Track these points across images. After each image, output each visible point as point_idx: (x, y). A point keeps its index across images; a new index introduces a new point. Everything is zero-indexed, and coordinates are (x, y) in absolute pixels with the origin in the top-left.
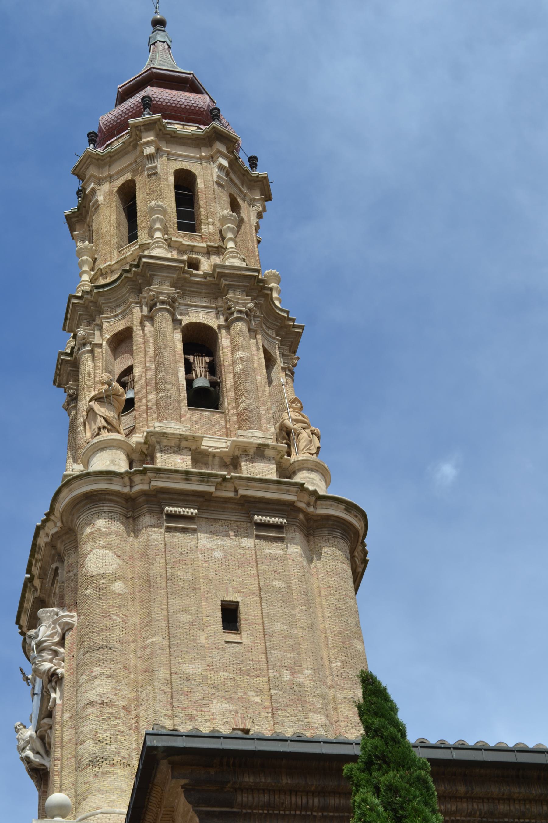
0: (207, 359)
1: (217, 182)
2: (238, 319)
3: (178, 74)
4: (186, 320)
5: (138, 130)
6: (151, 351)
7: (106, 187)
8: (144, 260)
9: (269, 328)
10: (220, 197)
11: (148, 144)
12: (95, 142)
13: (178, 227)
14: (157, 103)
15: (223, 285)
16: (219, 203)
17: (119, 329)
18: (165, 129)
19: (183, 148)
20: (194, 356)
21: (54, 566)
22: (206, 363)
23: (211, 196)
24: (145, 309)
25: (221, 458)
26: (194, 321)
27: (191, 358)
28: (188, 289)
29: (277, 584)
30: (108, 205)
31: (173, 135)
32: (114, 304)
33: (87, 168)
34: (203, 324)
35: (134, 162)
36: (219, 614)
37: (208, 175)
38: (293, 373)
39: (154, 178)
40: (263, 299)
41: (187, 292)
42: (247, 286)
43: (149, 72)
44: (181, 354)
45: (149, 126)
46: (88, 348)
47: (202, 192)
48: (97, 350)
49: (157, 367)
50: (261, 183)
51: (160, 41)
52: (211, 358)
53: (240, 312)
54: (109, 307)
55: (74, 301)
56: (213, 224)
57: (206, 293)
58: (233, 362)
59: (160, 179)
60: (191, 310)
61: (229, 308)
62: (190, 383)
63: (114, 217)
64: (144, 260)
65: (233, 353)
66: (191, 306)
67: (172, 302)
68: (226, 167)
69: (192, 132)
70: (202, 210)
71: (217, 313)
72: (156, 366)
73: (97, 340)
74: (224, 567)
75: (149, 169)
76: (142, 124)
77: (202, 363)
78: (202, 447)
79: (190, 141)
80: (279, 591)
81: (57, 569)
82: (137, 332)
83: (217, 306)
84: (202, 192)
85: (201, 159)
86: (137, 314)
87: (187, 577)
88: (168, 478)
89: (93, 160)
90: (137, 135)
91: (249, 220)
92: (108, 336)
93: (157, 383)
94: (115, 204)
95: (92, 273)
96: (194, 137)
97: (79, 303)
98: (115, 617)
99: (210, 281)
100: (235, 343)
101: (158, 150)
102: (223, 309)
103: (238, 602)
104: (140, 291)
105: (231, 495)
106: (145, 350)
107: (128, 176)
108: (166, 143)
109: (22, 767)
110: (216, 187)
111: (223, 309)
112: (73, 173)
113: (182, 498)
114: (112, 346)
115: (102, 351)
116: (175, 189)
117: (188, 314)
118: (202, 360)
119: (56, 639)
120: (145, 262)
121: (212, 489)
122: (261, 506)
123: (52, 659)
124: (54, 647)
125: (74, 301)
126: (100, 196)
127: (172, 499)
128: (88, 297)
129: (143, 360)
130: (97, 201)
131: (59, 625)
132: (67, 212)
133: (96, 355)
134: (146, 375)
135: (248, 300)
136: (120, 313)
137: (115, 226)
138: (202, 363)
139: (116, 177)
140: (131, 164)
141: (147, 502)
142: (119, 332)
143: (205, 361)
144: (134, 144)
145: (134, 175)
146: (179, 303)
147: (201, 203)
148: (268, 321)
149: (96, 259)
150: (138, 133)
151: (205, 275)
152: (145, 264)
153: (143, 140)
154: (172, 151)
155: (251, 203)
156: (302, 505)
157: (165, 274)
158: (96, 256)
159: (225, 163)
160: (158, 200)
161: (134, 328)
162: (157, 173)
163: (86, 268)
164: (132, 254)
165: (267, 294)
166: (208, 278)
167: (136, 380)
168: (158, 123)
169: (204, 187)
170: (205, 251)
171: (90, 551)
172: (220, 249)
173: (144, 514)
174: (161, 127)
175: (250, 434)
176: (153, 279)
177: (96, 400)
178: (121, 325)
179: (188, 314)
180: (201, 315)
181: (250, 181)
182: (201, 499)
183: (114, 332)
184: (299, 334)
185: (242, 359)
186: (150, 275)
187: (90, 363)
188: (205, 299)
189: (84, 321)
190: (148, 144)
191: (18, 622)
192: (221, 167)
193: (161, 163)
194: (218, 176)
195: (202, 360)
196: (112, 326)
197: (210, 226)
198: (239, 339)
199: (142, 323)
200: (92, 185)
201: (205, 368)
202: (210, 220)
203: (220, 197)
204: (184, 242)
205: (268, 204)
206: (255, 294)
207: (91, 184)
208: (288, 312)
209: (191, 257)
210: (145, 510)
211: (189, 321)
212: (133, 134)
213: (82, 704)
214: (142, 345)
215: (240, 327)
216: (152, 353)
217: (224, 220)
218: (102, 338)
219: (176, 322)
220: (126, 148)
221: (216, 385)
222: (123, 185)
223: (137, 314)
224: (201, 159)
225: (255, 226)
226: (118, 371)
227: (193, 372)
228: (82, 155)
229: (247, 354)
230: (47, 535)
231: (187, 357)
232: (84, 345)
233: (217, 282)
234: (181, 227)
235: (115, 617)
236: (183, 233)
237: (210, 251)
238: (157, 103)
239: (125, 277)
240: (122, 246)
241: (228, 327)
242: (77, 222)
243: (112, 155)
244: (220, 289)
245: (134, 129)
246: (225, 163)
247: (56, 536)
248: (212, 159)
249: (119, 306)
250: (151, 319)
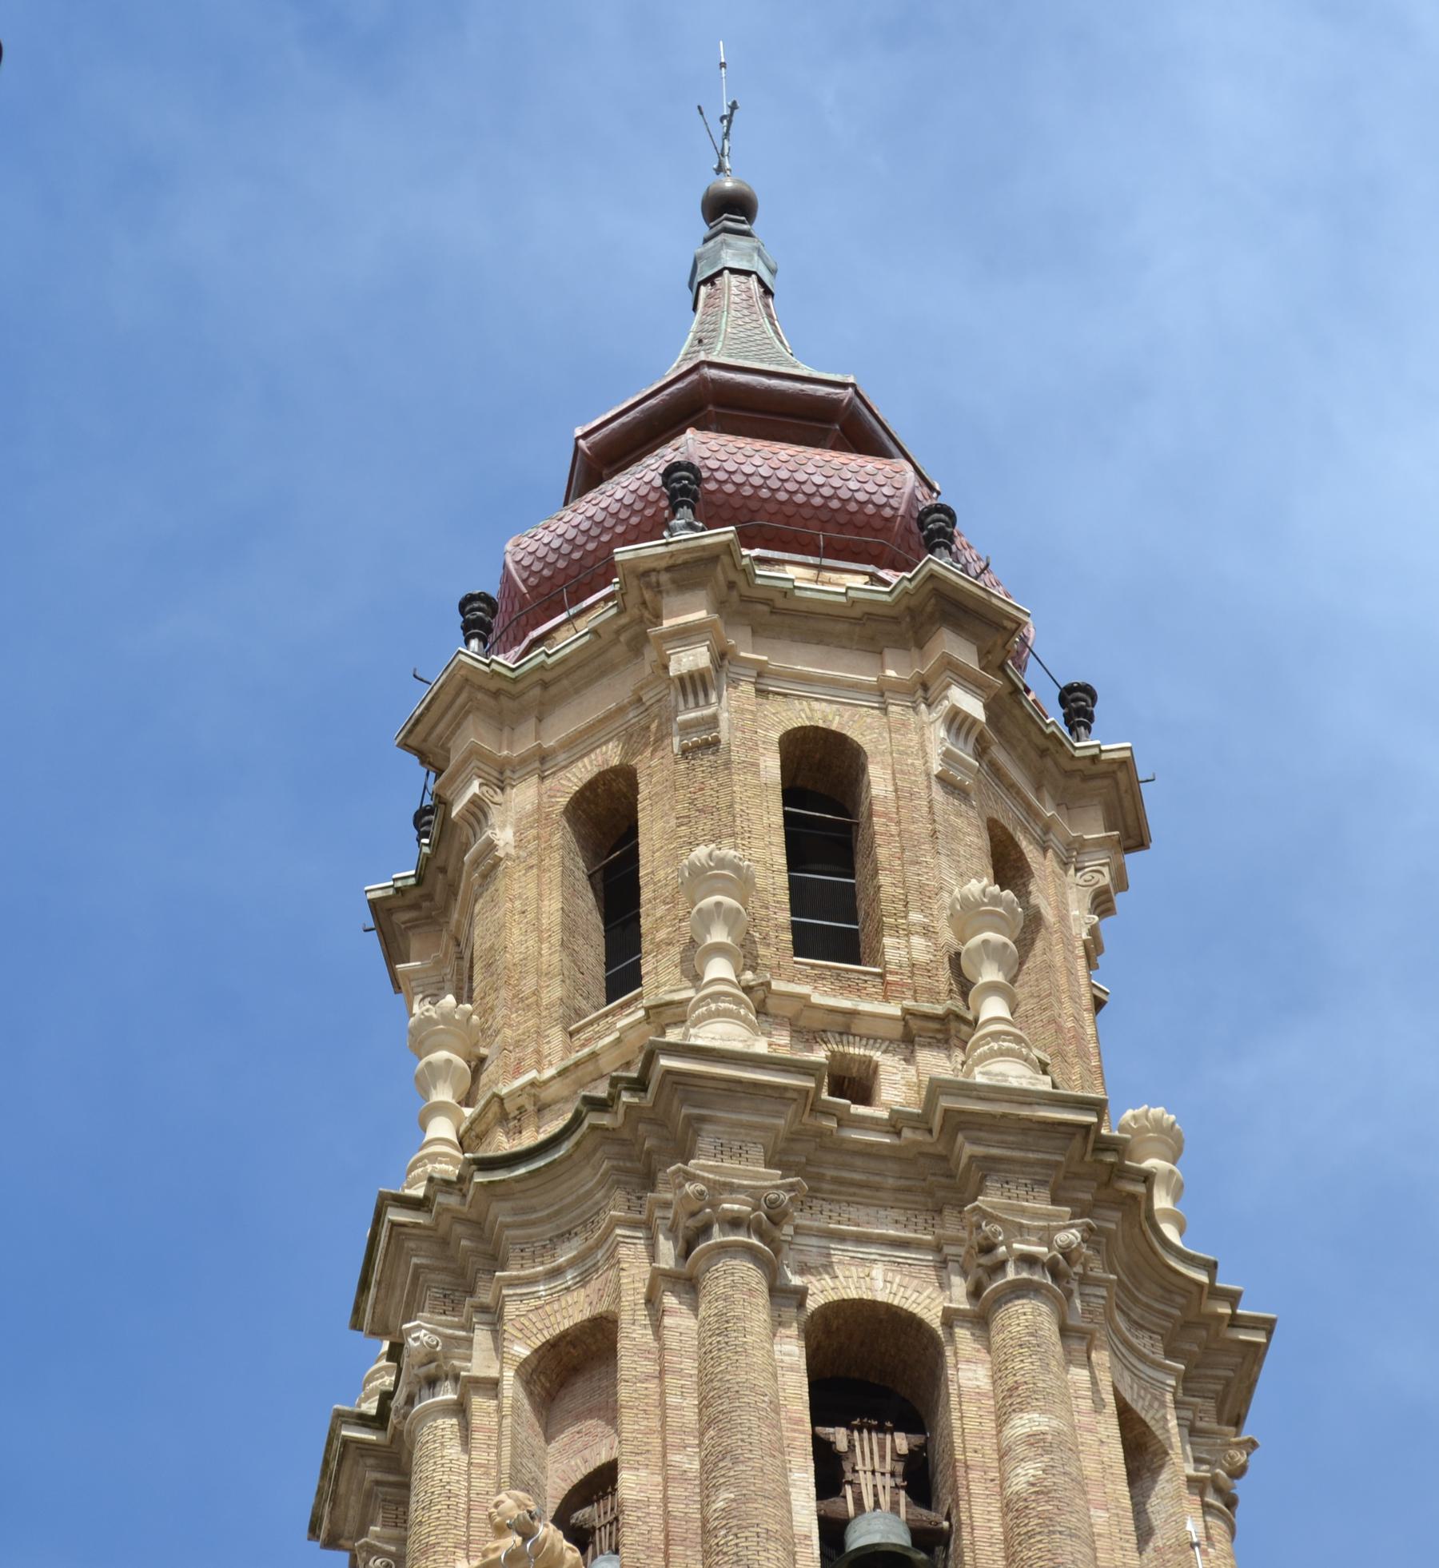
0: (902, 1442)
1: (941, 779)
2: (1020, 1290)
3: (798, 386)
4: (821, 1292)
5: (649, 586)
6: (685, 1406)
7: (524, 795)
8: (665, 1062)
9: (1142, 1327)
10: (954, 835)
11: (685, 635)
12: (489, 630)
13: (794, 942)
14: (720, 490)
15: (964, 1160)
16: (952, 854)
17: (567, 1324)
18: (750, 584)
19: (816, 651)
20: (851, 1428)
22: (897, 1457)
23: (922, 828)
24: (667, 1249)
26: (853, 1294)
27: (839, 1437)
28: (831, 1173)
30: (533, 861)
31: (780, 603)
32: (549, 1230)
34: (888, 1307)
35: (631, 703)
37: (908, 753)
38: (1231, 1502)
39: (707, 759)
40: (1118, 1215)
41: (825, 1186)
42: (1056, 1165)
43: (694, 377)
44: (799, 1421)
45: (690, 572)
46: (447, 1394)
47: (885, 815)
48: (480, 1404)
49: (708, 1468)
50: (1106, 782)
51: (733, 271)
52: (917, 1439)
53: (1029, 1260)
54: (529, 1240)
55: (395, 1215)
56: (927, 932)
58: (1003, 1454)
59: (728, 764)
60: (839, 1253)
61: (988, 1248)
62: (832, 1531)
63: (553, 906)
64: (665, 1062)
65: (1002, 1419)
66: (841, 1237)
67: (769, 1222)
68: (975, 721)
69: (851, 593)
70: (884, 879)
71: (942, 1265)
72: (703, 1464)
73: (480, 1363)
75: (686, 728)
76: (663, 564)
77: (883, 1457)
79: (841, 627)
82: (634, 1334)
83: (939, 1238)
84: (885, 815)
85: (882, 692)
86: (634, 1268)
89: (480, 696)
90: (644, 603)
91: (1063, 918)
92: (521, 1351)
93: (706, 1532)
94: (557, 856)
95: (468, 1112)
96: (857, 612)
97: (416, 1225)
99: (915, 1143)
100: (1011, 1380)
101: (722, 657)
102: (962, 1251)
104: (649, 1181)
106: (663, 1405)
107: (610, 755)
108: (754, 633)
110: (938, 794)
111: (962, 1251)
112: (404, 745)
114: (537, 1389)
115: (499, 1409)
116: (785, 804)
117: (828, 1267)
118: (882, 1446)
120: (669, 1072)
125: (395, 1215)
126: (503, 827)
128: (451, 1201)
129: (656, 1441)
130: (491, 846)
132: (378, 888)
133: (476, 1421)
134: (666, 1499)
135: (1058, 1217)
136: (572, 1263)
137: (556, 938)
138: (883, 1457)
139: (562, 758)
140: (621, 710)
142: (563, 1336)
143: (893, 1449)
144: (635, 637)
145: (630, 751)
146: (797, 1228)
147: (883, 853)
148: (1136, 1300)
149: (482, 1060)
150: (648, 595)
151: (896, 1123)
152: (670, 1078)
153: (667, 623)
154: (775, 664)
155: (1071, 856)
157: (744, 1118)
158: (483, 1051)
159: (974, 707)
160: (718, 843)
161: (625, 1318)
162: (716, 742)
163: (443, 1094)
164: (618, 1040)
165: (1133, 1197)
166: (907, 1133)
167: (629, 1517)
168: (725, 559)
169: (892, 796)
170: (897, 1030)
172: (953, 1025)
174: (733, 576)
176: (697, 1133)
178: (572, 1309)
179: (828, 1267)
180: (878, 1271)
181: (1068, 774)
183: (547, 1335)
184: (1256, 1353)
185: (1035, 1440)
186: (688, 1117)
187: (453, 1451)
188: (894, 1214)
189: (435, 1292)
190: (685, 635)
192: (957, 721)
193: (731, 705)
194: (947, 756)
195: (882, 1446)
196: (542, 1312)
197: (916, 940)
198: (1024, 1367)
199: (652, 1301)
200: (475, 788)
201: (893, 1474)
202: (915, 917)
203: (954, 835)
204: (817, 999)
205: (1132, 860)
206: (1088, 1197)
207: (467, 783)
208: (1211, 1267)
209: (844, 1055)
211: (833, 1296)
212: (632, 598)
214: (653, 1385)
215: (1028, 1318)
216: (691, 1417)
217: (967, 915)
218: (500, 1356)
219: (784, 1297)
220: (602, 651)
222: (591, 786)
223: (634, 1268)
225: (1085, 944)
227: (848, 1488)
228: (437, 677)
229: (1054, 1423)
231: (825, 1431)
232: (432, 1382)
233: (940, 1149)
234: (806, 943)
236: (813, 966)
237: (911, 1035)
238: (720, 490)
239: (593, 1128)
240: (579, 1014)
241: (981, 1321)
242: (413, 925)
243: (548, 676)
244: (950, 1176)
245: (633, 582)
246: (974, 707)
248: (924, 691)
249: (566, 1235)
250: (689, 1285)
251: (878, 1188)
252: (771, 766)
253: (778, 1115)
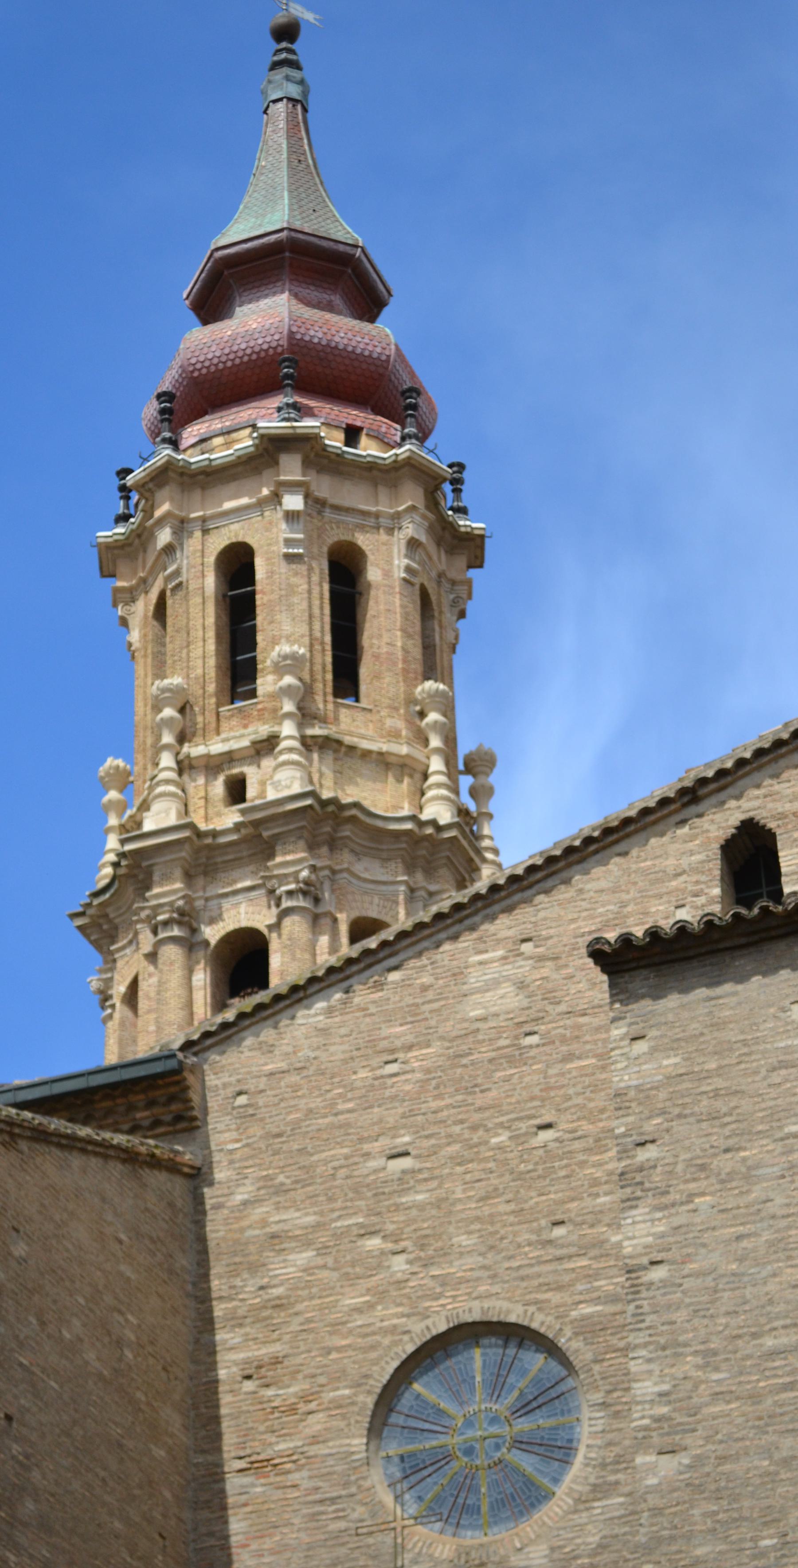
9: (390, 860)
14: (201, 374)
16: (290, 607)
31: (209, 470)
42: (302, 827)
43: (212, 260)
53: (290, 893)
57: (250, 856)
60: (226, 904)
66: (226, 895)
76: (148, 479)
79: (240, 469)
85: (261, 504)
89: (116, 552)
96: (244, 459)
139: (150, 579)
148: (382, 850)
153: (158, 513)
154: (209, 512)
157: (168, 858)
170: (252, 752)
176: (149, 874)
188: (252, 868)
192: (291, 516)
209: (232, 776)
224: (261, 504)
238: (201, 374)
245: (142, 490)
251: (241, 858)
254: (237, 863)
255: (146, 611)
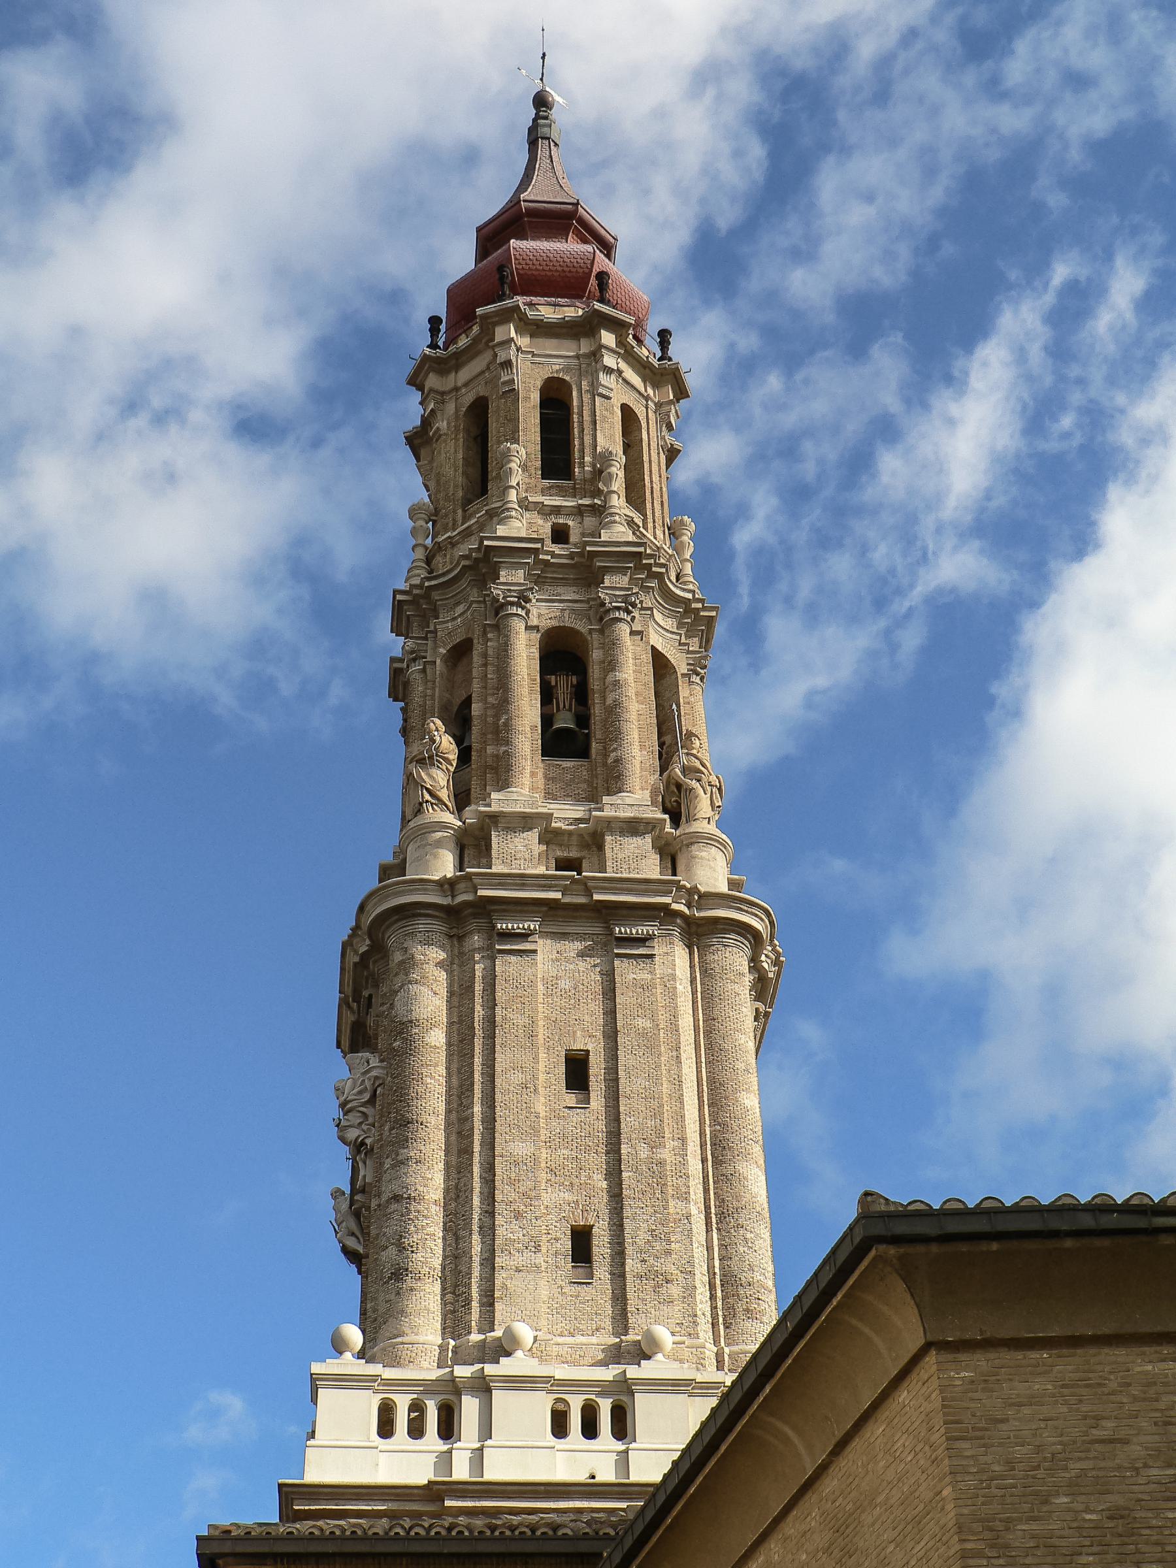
19: (554, 342)
21: (366, 993)
25: (581, 835)
29: (641, 1023)
33: (427, 375)
36: (562, 1069)
55: (399, 597)
62: (547, 720)
64: (486, 543)
74: (572, 1001)
75: (504, 383)
78: (553, 825)
79: (564, 330)
80: (643, 1034)
81: (370, 996)
87: (521, 1020)
88: (500, 884)
98: (429, 1081)
103: (588, 1051)
105: (582, 900)
109: (338, 1247)
112: (409, 383)
113: (519, 908)
119: (366, 1096)
121: (558, 895)
122: (625, 912)
123: (361, 1124)
124: (362, 1109)
127: (505, 911)
131: (369, 1079)
136: (460, 616)
140: (483, 372)
141: (475, 916)
156: (681, 907)
161: (475, 641)
165: (661, 573)
171: (401, 987)
173: (471, 932)
175: (619, 802)
177: (417, 762)
182: (545, 909)
188: (574, 589)
191: (339, 1046)
210: (472, 927)
213: (384, 1198)
221: (583, 720)
226: (457, 701)
230: (356, 952)
235: (429, 1081)
247: (365, 957)
249: (458, 604)
252: (536, 397)
253: (529, 558)
254: (564, 582)
255: (457, 410)
